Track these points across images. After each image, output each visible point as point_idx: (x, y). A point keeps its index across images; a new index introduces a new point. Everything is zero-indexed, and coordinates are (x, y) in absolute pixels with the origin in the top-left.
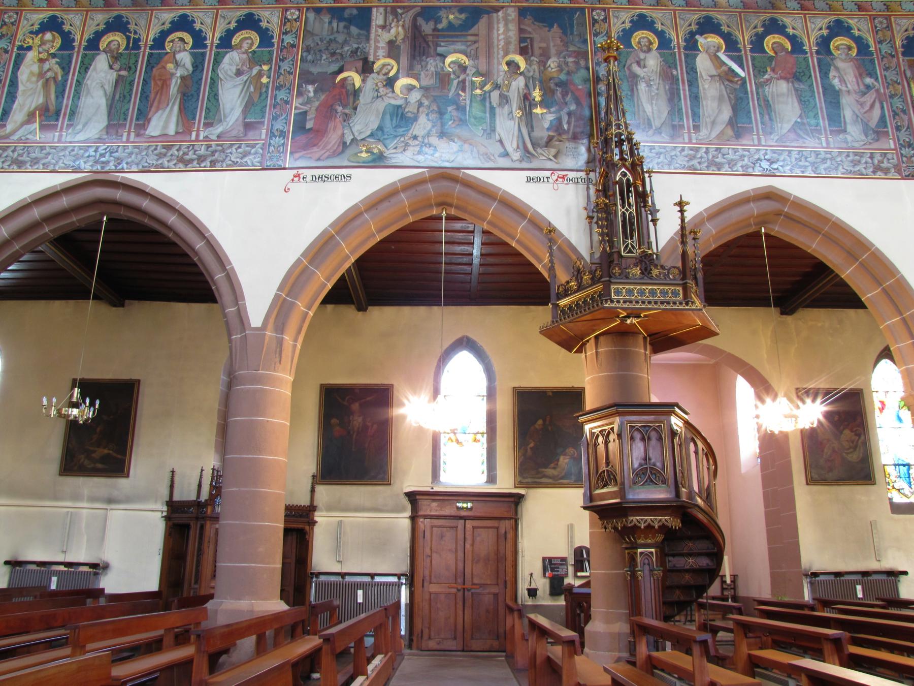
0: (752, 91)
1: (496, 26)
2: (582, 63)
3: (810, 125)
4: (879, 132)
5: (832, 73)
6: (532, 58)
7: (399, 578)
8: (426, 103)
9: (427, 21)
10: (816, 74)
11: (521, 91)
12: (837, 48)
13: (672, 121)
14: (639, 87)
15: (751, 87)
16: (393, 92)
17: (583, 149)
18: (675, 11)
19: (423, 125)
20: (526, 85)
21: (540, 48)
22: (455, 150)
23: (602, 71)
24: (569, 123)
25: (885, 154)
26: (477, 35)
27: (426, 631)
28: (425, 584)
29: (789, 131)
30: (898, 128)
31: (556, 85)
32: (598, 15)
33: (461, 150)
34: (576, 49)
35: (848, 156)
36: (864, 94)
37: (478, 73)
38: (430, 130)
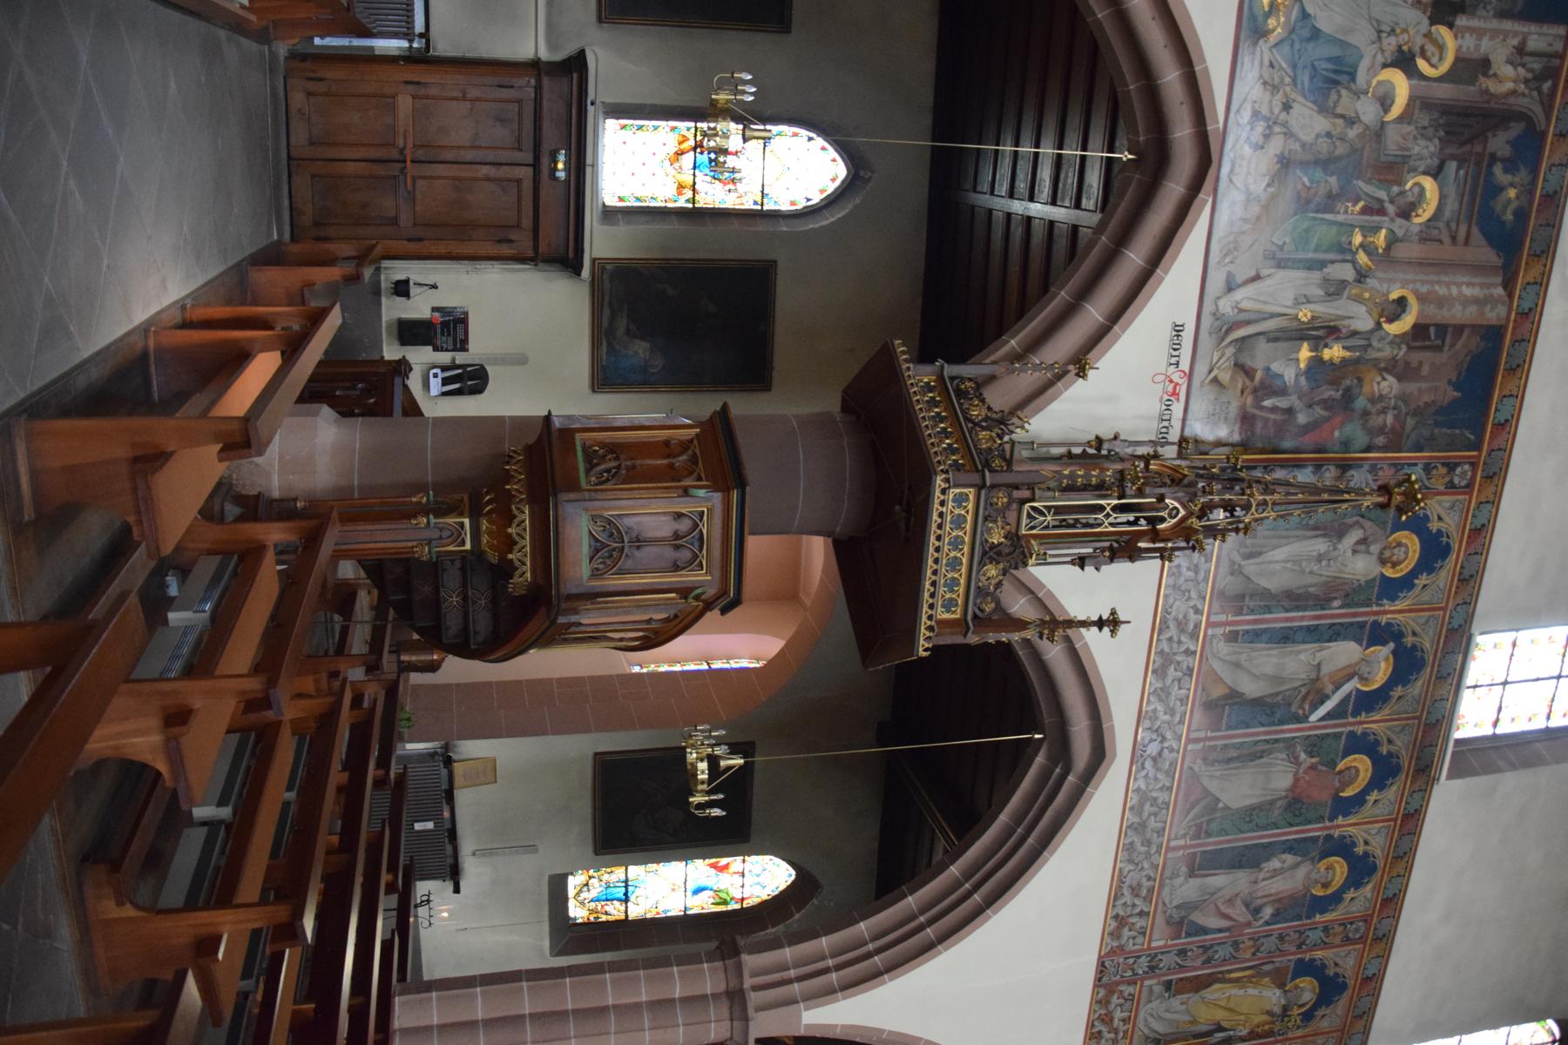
0: (1283, 731)
1: (1477, 280)
2: (1380, 441)
3: (1209, 821)
4: (1182, 924)
5: (1290, 859)
6: (1404, 348)
7: (421, 36)
8: (1352, 133)
9: (1515, 144)
10: (1291, 834)
11: (1346, 322)
12: (1329, 868)
13: (1252, 596)
14: (1321, 540)
15: (1290, 731)
16: (1385, 66)
17: (1222, 432)
18: (1444, 609)
19: (1309, 123)
20: (1355, 333)
21: (1421, 363)
22: (1252, 187)
23: (1358, 478)
24: (1274, 409)
25: (1144, 934)
26: (1466, 242)
27: (321, 87)
28: (410, 87)
29: (1205, 789)
30: (1182, 953)
31: (1348, 390)
32: (1464, 473)
33: (1250, 198)
34: (1407, 430)
35: (1149, 878)
36: (1247, 906)
37: (1392, 241)
38: (1297, 139)
